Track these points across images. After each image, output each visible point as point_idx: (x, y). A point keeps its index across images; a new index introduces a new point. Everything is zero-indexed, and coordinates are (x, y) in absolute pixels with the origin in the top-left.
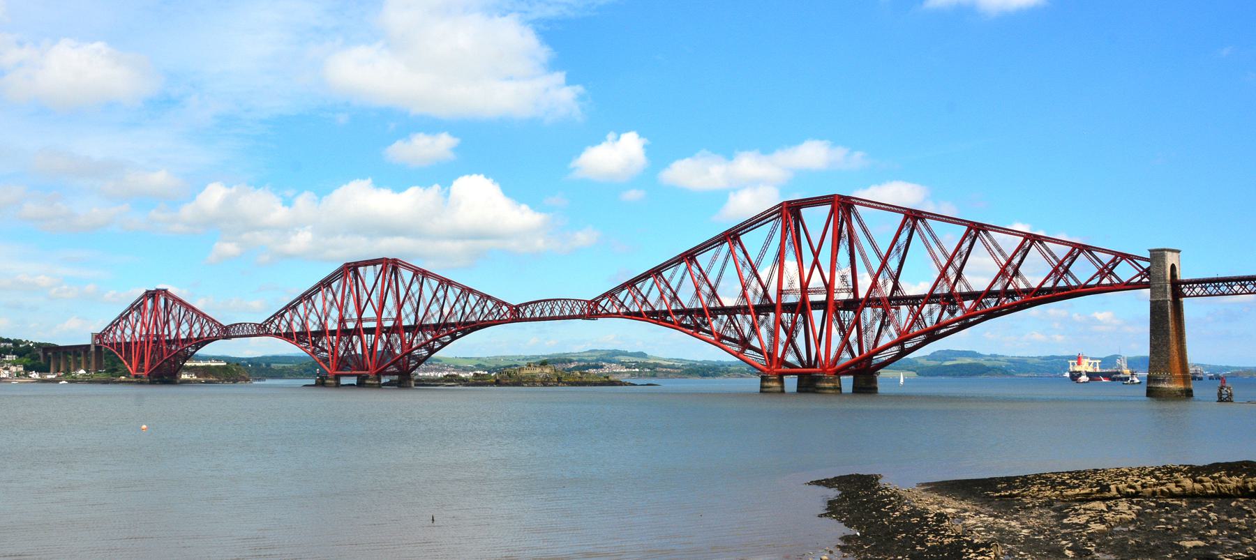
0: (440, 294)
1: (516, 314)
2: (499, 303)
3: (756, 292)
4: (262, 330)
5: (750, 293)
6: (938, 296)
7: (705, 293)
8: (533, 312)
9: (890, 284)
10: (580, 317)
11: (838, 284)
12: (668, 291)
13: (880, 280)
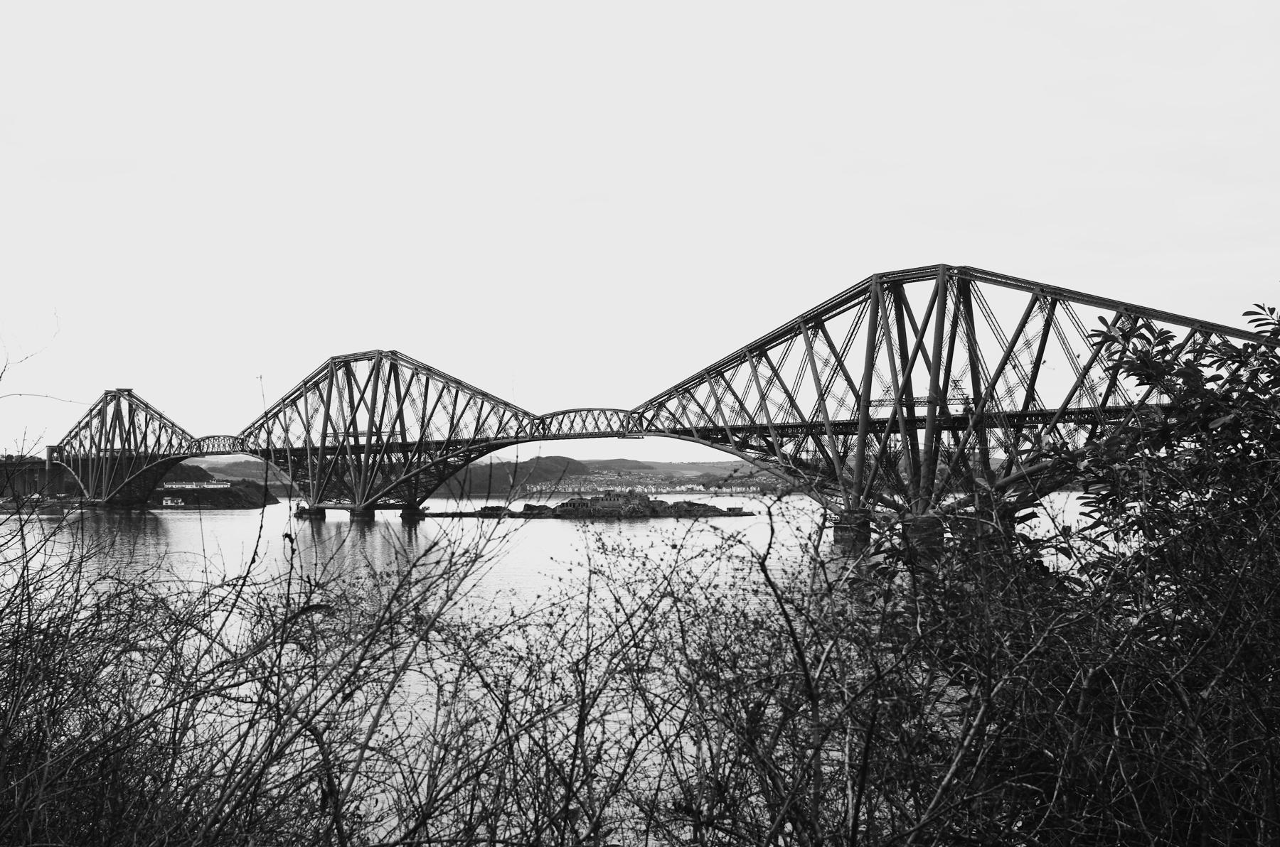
0: (447, 399)
1: (541, 428)
2: (517, 413)
3: (842, 402)
4: (239, 443)
5: (831, 404)
6: (1073, 412)
7: (774, 403)
8: (560, 428)
9: (1020, 395)
10: (612, 434)
11: (876, 393)
12: (729, 399)
13: (1000, 388)
